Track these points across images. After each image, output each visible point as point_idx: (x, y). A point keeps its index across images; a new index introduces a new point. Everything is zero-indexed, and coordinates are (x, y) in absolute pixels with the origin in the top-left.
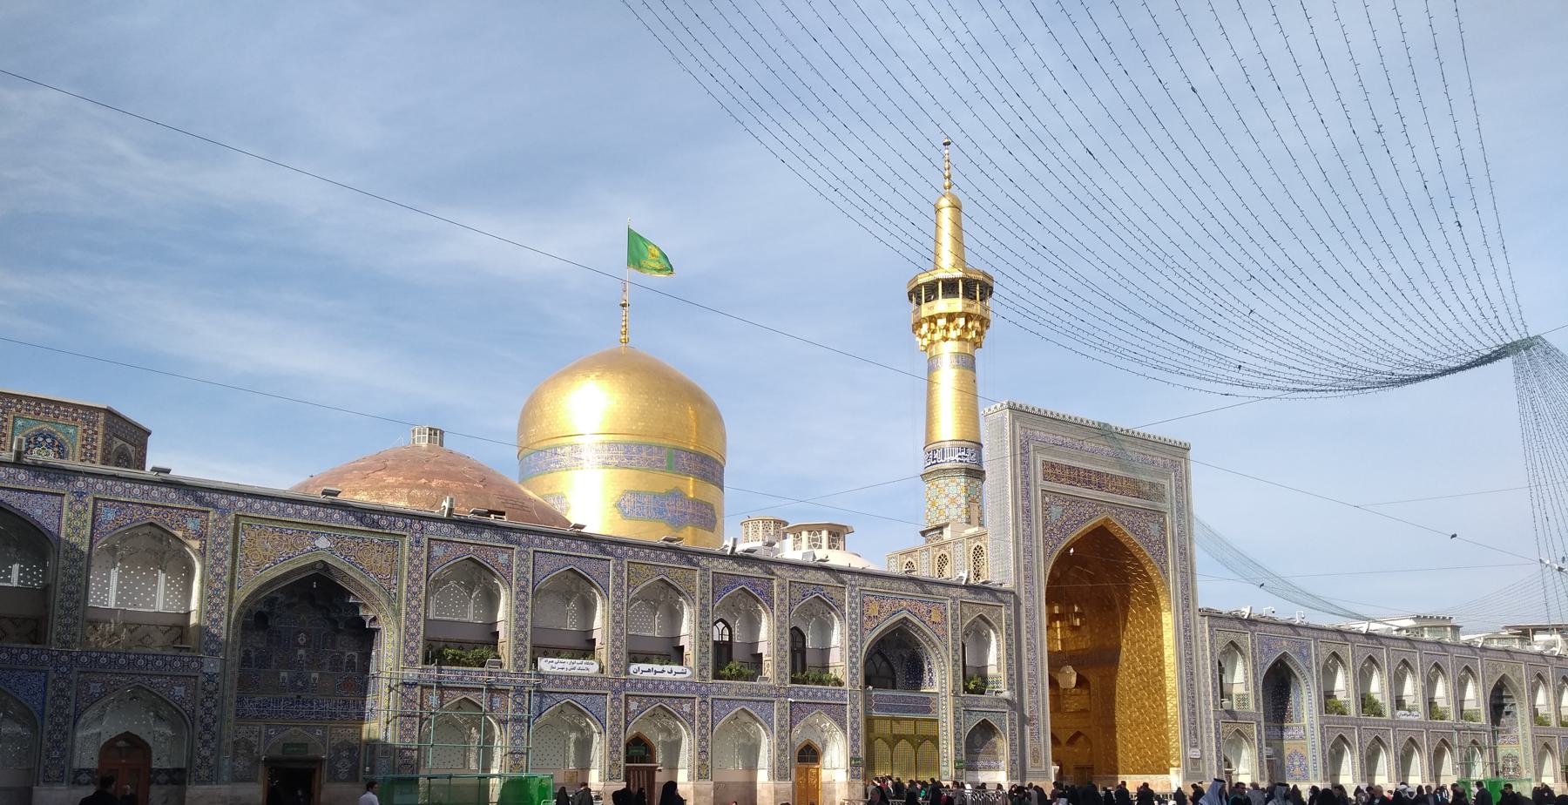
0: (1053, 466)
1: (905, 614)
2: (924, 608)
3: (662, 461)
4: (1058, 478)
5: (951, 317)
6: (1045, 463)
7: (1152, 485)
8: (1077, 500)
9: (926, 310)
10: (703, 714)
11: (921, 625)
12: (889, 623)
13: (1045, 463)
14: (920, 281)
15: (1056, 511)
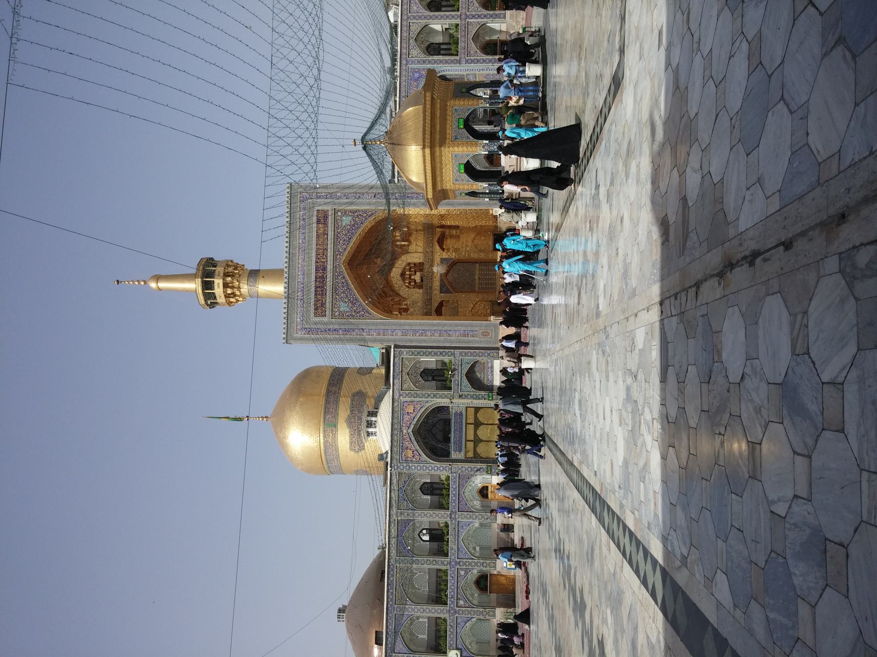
0: (316, 309)
1: (410, 431)
2: (407, 418)
3: (332, 431)
4: (323, 305)
5: (226, 286)
6: (316, 315)
7: (318, 222)
8: (335, 289)
9: (221, 299)
10: (465, 564)
11: (416, 420)
12: (415, 443)
13: (316, 315)
14: (203, 302)
15: (344, 307)
